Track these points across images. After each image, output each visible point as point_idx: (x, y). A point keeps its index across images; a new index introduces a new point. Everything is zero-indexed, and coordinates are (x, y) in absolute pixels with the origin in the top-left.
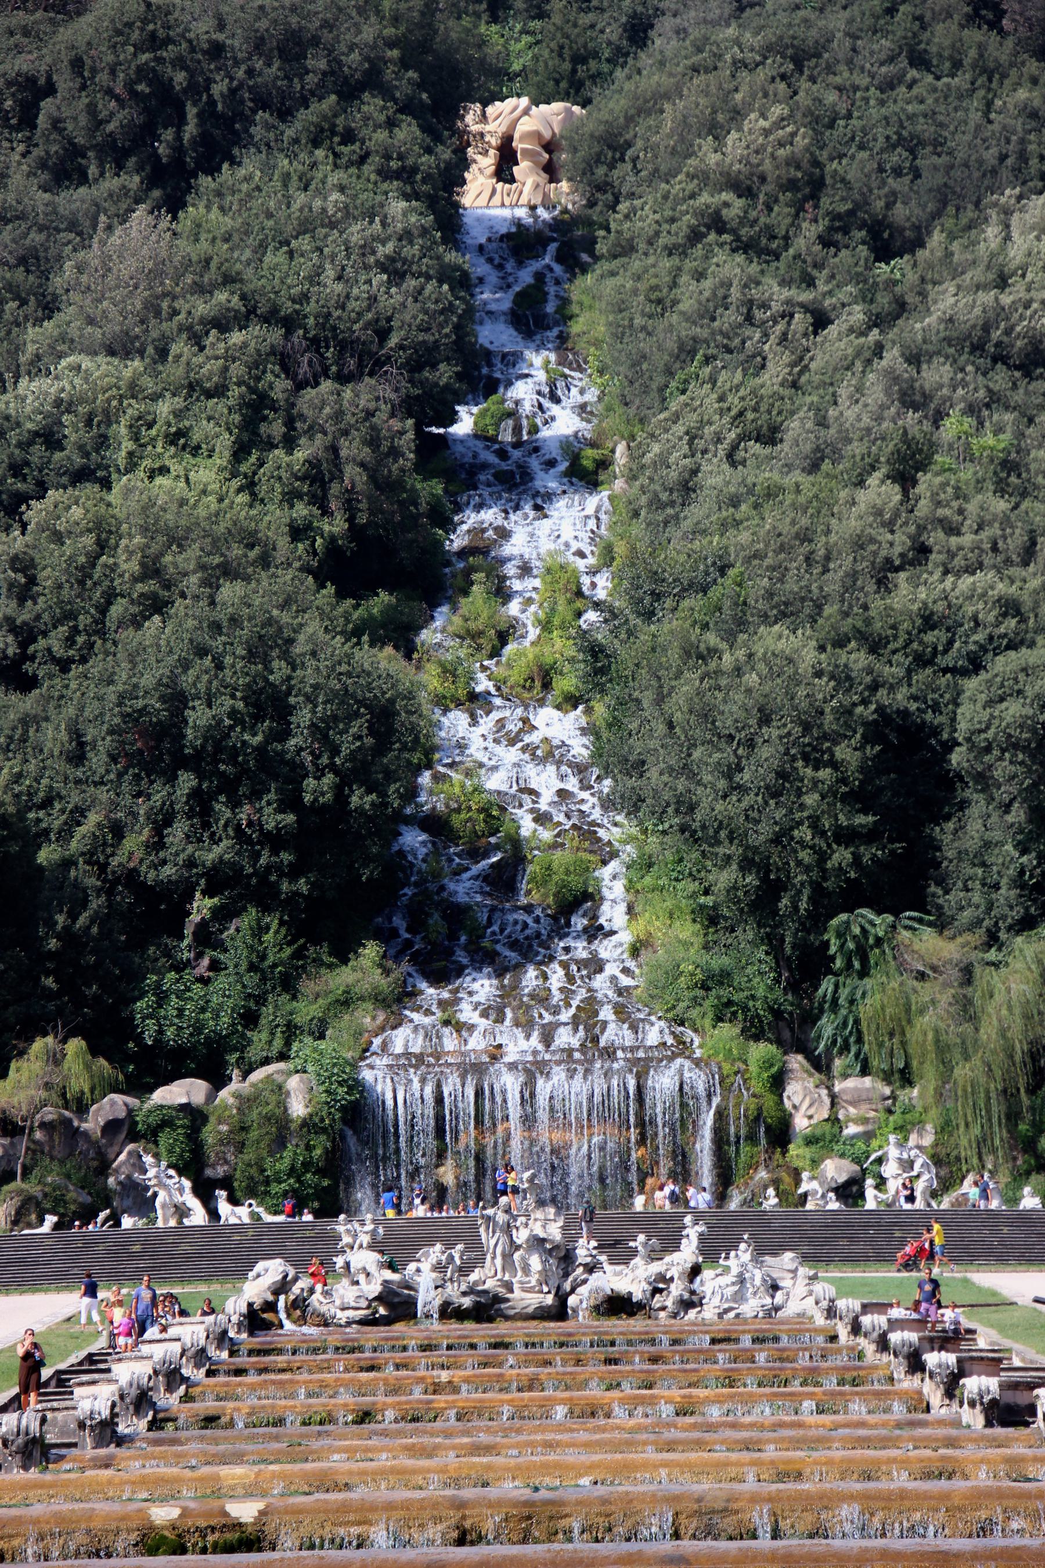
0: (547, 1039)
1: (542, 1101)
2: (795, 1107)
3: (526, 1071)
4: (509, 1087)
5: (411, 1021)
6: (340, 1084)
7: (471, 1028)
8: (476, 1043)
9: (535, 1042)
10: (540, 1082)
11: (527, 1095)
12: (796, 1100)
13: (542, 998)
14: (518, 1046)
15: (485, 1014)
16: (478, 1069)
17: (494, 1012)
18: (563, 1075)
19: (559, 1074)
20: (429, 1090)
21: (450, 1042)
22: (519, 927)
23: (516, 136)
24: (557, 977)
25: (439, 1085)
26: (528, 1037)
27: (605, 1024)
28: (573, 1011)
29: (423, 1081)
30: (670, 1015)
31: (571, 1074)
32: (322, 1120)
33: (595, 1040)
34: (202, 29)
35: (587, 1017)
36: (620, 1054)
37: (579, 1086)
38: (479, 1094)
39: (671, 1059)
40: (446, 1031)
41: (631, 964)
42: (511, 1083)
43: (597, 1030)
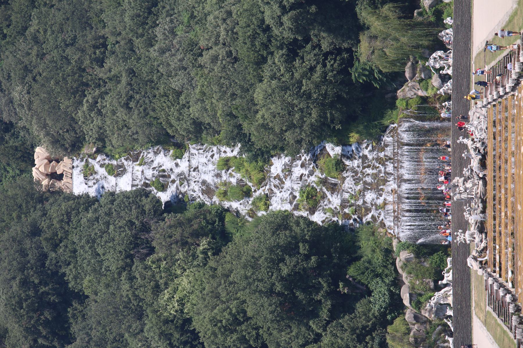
3: (401, 182)
5: (382, 220)
7: (385, 199)
8: (390, 198)
11: (409, 182)
12: (413, 94)
13: (375, 176)
14: (392, 185)
15: (381, 195)
16: (400, 198)
17: (379, 192)
18: (402, 170)
19: (403, 171)
20: (407, 214)
21: (390, 207)
23: (46, 172)
24: (369, 171)
25: (404, 211)
27: (385, 156)
28: (380, 165)
29: (404, 216)
31: (402, 167)
33: (390, 159)
34: (15, 285)
35: (382, 162)
36: (395, 151)
38: (408, 198)
39: (398, 134)
42: (405, 186)
43: (387, 158)
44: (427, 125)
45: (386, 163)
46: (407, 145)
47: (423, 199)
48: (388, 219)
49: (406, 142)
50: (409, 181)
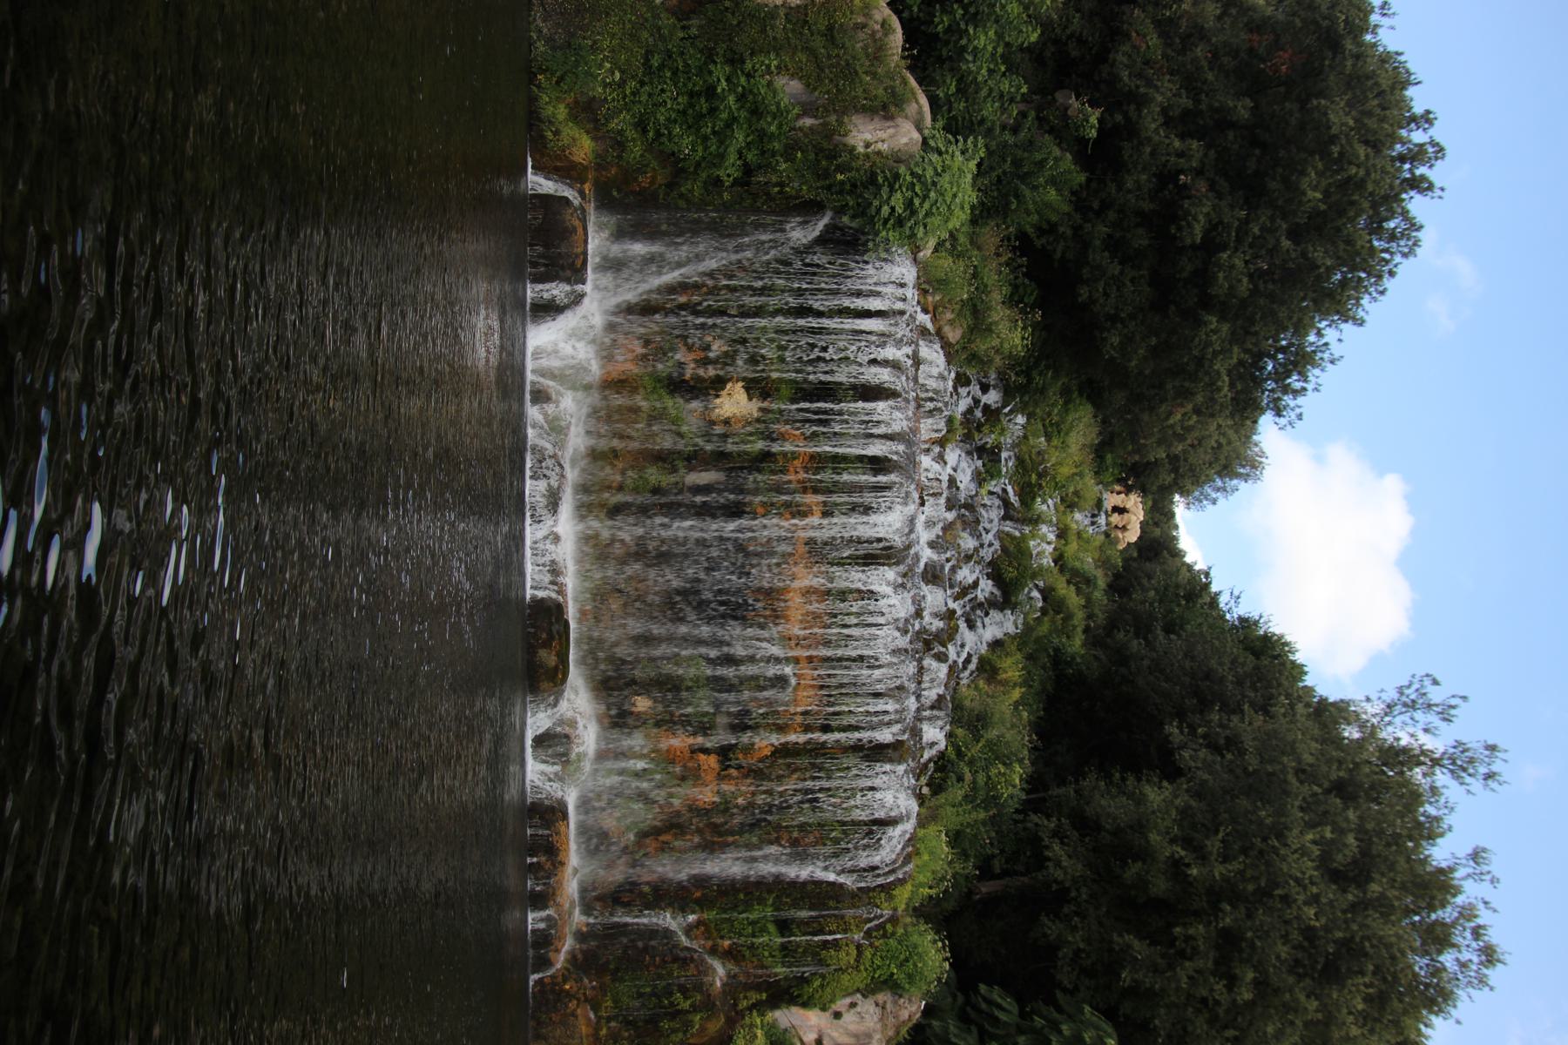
0: (933, 575)
1: (855, 578)
2: (837, 1015)
6: (909, 204)
9: (927, 554)
10: (890, 574)
12: (849, 1018)
20: (884, 376)
21: (929, 428)
22: (988, 526)
26: (932, 545)
29: (895, 365)
37: (887, 639)
38: (878, 464)
40: (942, 425)
41: (972, 666)
42: (887, 523)
44: (773, 864)
45: (941, 624)
46: (876, 753)
47: (795, 455)
49: (888, 767)
50: (876, 555)
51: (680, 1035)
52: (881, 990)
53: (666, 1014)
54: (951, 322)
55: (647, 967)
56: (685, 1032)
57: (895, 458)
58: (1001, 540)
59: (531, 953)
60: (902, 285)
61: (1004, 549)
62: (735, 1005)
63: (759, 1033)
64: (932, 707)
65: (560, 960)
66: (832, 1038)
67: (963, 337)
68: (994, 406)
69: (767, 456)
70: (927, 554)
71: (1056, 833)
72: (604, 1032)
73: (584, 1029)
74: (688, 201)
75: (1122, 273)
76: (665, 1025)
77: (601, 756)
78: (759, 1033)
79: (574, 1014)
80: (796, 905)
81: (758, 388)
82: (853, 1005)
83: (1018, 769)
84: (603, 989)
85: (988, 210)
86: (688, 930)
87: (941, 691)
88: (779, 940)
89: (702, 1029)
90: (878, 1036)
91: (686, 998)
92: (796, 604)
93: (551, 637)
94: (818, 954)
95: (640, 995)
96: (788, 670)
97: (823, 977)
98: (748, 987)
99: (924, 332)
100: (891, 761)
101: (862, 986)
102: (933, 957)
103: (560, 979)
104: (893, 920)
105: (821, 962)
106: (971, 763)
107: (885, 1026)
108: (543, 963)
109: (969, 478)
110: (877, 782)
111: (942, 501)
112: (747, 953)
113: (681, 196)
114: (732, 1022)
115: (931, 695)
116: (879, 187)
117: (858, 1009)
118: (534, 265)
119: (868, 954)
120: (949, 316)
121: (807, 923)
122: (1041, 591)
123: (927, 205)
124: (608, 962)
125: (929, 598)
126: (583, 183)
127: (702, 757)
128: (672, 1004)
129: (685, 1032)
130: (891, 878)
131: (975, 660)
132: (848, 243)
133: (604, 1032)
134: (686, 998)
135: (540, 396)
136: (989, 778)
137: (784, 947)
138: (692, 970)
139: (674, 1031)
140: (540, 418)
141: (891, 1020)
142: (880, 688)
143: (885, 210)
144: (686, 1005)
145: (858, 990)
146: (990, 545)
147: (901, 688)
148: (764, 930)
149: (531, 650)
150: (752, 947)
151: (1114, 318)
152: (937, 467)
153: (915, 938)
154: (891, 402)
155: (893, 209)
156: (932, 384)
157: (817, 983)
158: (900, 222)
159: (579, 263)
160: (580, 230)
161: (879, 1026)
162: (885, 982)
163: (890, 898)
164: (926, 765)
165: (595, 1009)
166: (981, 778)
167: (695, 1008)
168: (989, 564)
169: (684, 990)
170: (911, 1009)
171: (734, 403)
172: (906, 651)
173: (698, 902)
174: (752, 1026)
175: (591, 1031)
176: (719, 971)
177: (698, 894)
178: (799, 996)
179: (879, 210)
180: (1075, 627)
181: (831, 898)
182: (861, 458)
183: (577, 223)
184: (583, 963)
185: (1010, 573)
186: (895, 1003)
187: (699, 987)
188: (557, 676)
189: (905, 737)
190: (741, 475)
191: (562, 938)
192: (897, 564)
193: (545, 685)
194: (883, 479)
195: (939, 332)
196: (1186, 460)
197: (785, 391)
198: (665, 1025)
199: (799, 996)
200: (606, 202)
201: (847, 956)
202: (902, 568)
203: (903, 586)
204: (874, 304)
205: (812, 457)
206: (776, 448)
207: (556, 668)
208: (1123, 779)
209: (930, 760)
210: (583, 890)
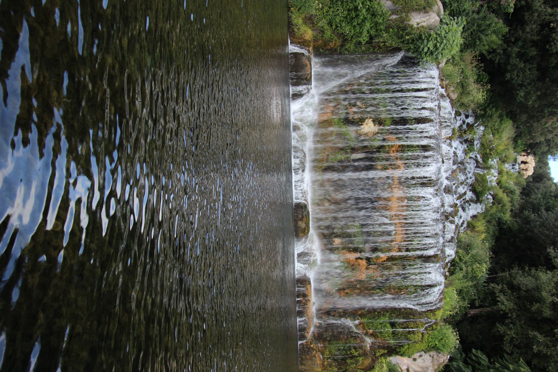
0: (448, 190)
2: (415, 360)
4: (426, 169)
6: (435, 46)
8: (445, 148)
9: (446, 182)
10: (430, 190)
12: (419, 361)
21: (446, 133)
22: (470, 171)
26: (447, 178)
29: (431, 110)
30: (457, 260)
32: (407, 34)
37: (429, 216)
38: (425, 148)
41: (465, 225)
42: (429, 171)
43: (451, 218)
45: (452, 209)
46: (427, 259)
47: (392, 146)
48: (447, 111)
49: (432, 265)
50: (426, 183)
51: (354, 365)
52: (432, 350)
53: (349, 357)
54: (453, 91)
55: (342, 339)
56: (356, 364)
57: (432, 145)
58: (475, 175)
59: (299, 333)
60: (433, 78)
61: (476, 179)
62: (375, 354)
63: (384, 365)
64: (449, 242)
65: (309, 335)
66: (413, 368)
67: (458, 97)
68: (471, 123)
69: (382, 147)
70: (446, 182)
71: (501, 291)
72: (326, 363)
73: (319, 362)
74: (348, 51)
75: (525, 66)
76: (349, 361)
77: (323, 261)
78: (384, 365)
79: (315, 356)
80: (397, 317)
81: (379, 122)
82: (421, 356)
83: (484, 265)
84: (325, 347)
85: (467, 46)
86: (356, 326)
87: (453, 235)
88: (391, 330)
89: (363, 363)
90: (431, 368)
91: (356, 351)
92: (394, 204)
93: (303, 217)
94: (406, 336)
95: (339, 350)
96: (392, 228)
97: (409, 345)
98: (380, 347)
99: (442, 96)
100: (433, 262)
101: (424, 349)
102: (452, 338)
103: (309, 343)
104: (436, 323)
105: (408, 339)
106: (465, 263)
107: (434, 365)
108: (303, 337)
109: (461, 152)
110: (428, 270)
111: (451, 162)
112: (379, 335)
113: (346, 49)
114: (374, 361)
115: (448, 236)
116: (423, 40)
117: (423, 357)
118: (292, 79)
119: (426, 336)
120: (452, 89)
121: (402, 324)
122: (492, 196)
123: (442, 46)
124: (326, 338)
125: (447, 199)
126: (309, 47)
127: (360, 261)
128: (351, 353)
129: (356, 364)
130: (434, 308)
131: (465, 223)
132: (410, 62)
133: (326, 363)
134: (356, 351)
135: (296, 128)
136: (473, 269)
137: (393, 333)
138: (358, 341)
139: (352, 363)
140: (297, 136)
141: (436, 362)
142: (429, 234)
143: (426, 50)
144: (356, 354)
145: (423, 350)
146: (471, 178)
147: (436, 234)
148: (385, 326)
149: (296, 221)
150: (381, 333)
151: (521, 85)
152: (449, 148)
153: (445, 331)
154: (429, 124)
155: (429, 48)
156: (446, 116)
157: (406, 347)
158: (432, 53)
159: (309, 77)
160: (309, 65)
161: (431, 364)
162: (433, 347)
163: (434, 315)
164: (447, 264)
165: (323, 354)
166: (470, 269)
167: (360, 355)
168: (470, 185)
169: (355, 348)
170: (444, 358)
171: (369, 127)
172: (438, 220)
173: (360, 315)
174: (382, 362)
175: (321, 362)
176: (369, 341)
177: (360, 312)
178: (399, 352)
179: (423, 49)
180: (506, 210)
181: (410, 314)
182: (418, 146)
183: (308, 62)
184: (319, 337)
185: (479, 189)
186: (438, 355)
187: (361, 347)
188: (305, 231)
189: (439, 253)
190: (372, 156)
191: (309, 328)
192: (434, 186)
193: (301, 235)
194: (427, 154)
195: (448, 95)
196: (553, 141)
197: (388, 122)
198: (349, 361)
199: (399, 352)
200: (318, 53)
201: (418, 337)
202: (436, 188)
203: (437, 194)
204: (423, 86)
205: (399, 146)
206: (385, 144)
207: (305, 228)
208: (530, 270)
209: (449, 262)
210: (318, 310)
